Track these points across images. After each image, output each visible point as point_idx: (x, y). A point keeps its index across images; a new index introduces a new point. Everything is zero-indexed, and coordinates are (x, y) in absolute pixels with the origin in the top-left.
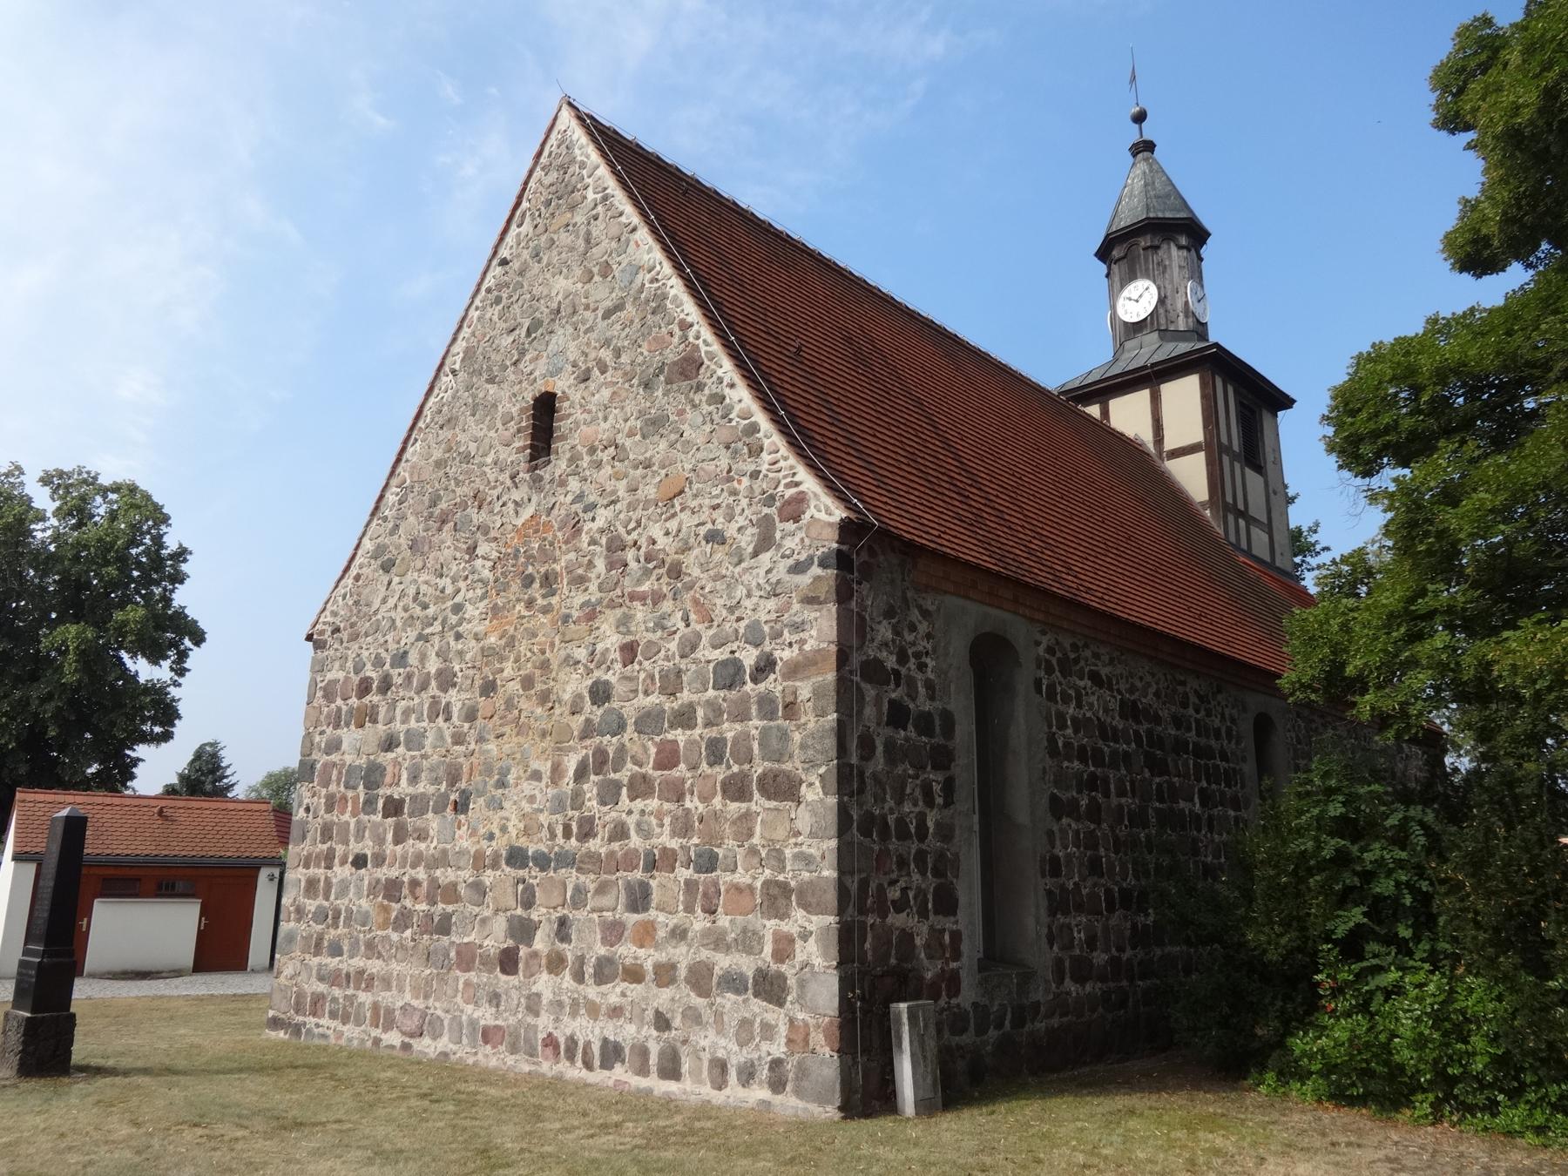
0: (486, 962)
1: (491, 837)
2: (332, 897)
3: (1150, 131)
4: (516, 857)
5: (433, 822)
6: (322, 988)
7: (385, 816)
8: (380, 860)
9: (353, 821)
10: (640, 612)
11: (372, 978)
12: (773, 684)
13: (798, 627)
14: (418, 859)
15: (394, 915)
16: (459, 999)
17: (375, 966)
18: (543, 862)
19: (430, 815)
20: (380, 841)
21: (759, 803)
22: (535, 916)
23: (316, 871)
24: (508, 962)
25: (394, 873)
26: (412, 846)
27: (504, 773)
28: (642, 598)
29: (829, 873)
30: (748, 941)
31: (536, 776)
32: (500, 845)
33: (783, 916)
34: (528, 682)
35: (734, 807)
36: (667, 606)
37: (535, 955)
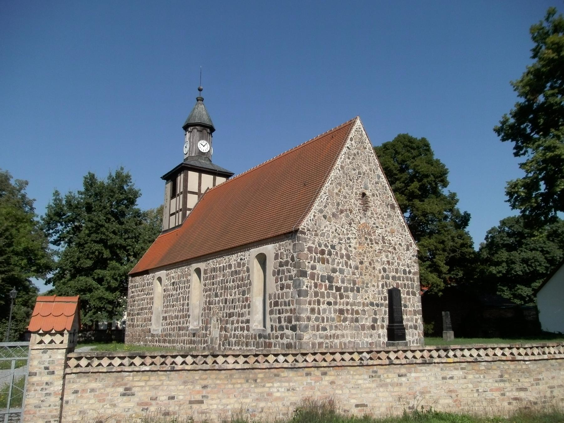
0: (369, 328)
1: (366, 299)
2: (321, 314)
3: (203, 94)
4: (372, 304)
5: (351, 294)
6: (322, 340)
7: (336, 291)
8: (336, 303)
9: (326, 292)
10: (390, 255)
11: (338, 335)
12: (411, 275)
13: (414, 266)
14: (347, 304)
15: (342, 318)
16: (363, 337)
17: (339, 332)
18: (377, 305)
19: (349, 292)
20: (336, 298)
21: (411, 296)
22: (377, 317)
23: (314, 306)
24: (373, 328)
25: (341, 307)
26: (345, 300)
27: (367, 284)
28: (390, 252)
29: (421, 308)
30: (412, 321)
31: (374, 286)
32: (368, 301)
33: (416, 316)
34: (370, 264)
35: (408, 297)
36: (394, 255)
37: (378, 325)
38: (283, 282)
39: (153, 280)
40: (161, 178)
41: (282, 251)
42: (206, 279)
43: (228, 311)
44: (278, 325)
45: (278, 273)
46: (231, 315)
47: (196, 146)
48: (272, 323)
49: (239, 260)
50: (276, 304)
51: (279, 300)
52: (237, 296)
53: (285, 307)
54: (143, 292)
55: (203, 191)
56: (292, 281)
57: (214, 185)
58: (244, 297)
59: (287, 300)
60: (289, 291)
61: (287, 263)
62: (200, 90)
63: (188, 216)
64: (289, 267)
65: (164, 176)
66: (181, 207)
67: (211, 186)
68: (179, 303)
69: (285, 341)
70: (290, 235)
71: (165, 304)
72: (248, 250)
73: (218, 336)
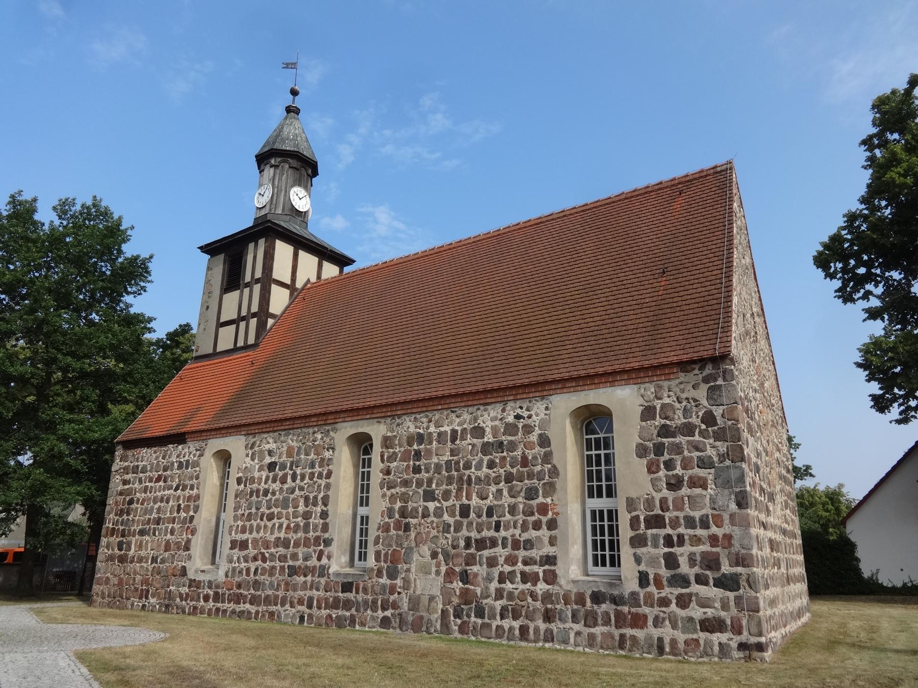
3: (299, 102)
38: (679, 471)
39: (201, 455)
40: (201, 248)
41: (667, 401)
42: (393, 458)
43: (474, 535)
44: (665, 573)
45: (659, 449)
46: (481, 544)
47: (285, 195)
48: (642, 567)
49: (510, 419)
50: (656, 522)
51: (667, 515)
52: (506, 500)
53: (690, 532)
54: (161, 483)
55: (299, 284)
56: (712, 471)
57: (319, 277)
58: (534, 503)
59: (697, 515)
60: (704, 492)
61: (688, 429)
62: (294, 93)
63: (271, 329)
64: (697, 437)
65: (207, 245)
66: (255, 308)
67: (313, 279)
68: (291, 510)
69: (696, 612)
70: (697, 367)
71: (240, 512)
72: (543, 398)
73: (436, 591)
